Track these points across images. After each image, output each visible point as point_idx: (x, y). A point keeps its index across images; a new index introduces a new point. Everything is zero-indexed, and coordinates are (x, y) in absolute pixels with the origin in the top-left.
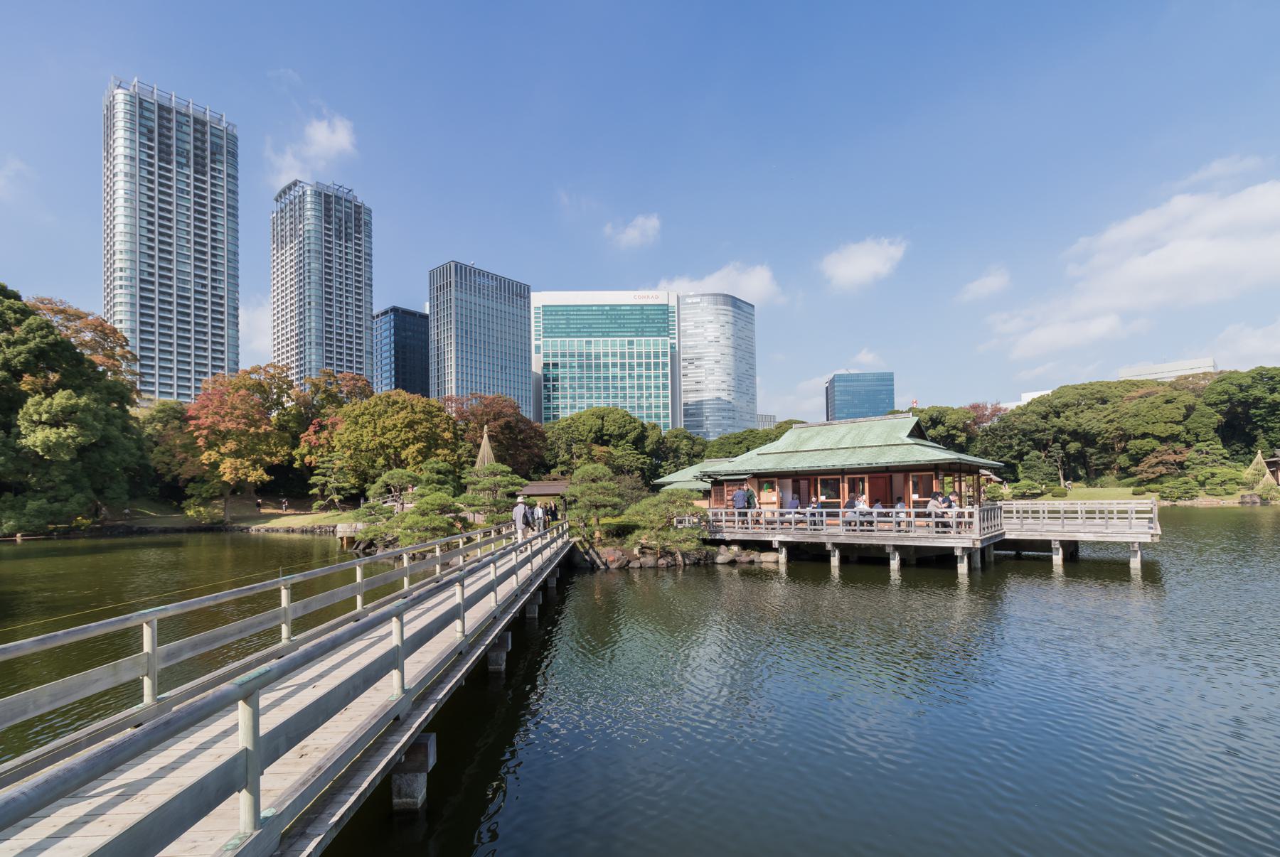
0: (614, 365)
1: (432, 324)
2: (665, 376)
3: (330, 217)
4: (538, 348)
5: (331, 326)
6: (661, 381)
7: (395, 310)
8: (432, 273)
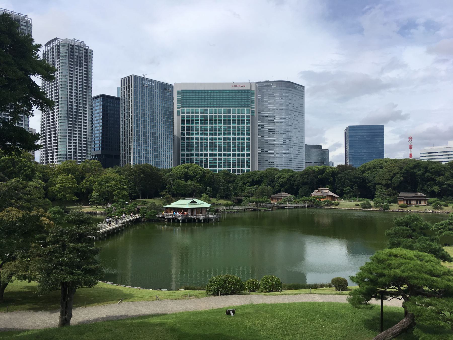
0: (220, 122)
1: (122, 105)
2: (248, 128)
3: (72, 55)
4: (179, 113)
5: (71, 108)
6: (245, 131)
7: (103, 96)
8: (122, 80)
